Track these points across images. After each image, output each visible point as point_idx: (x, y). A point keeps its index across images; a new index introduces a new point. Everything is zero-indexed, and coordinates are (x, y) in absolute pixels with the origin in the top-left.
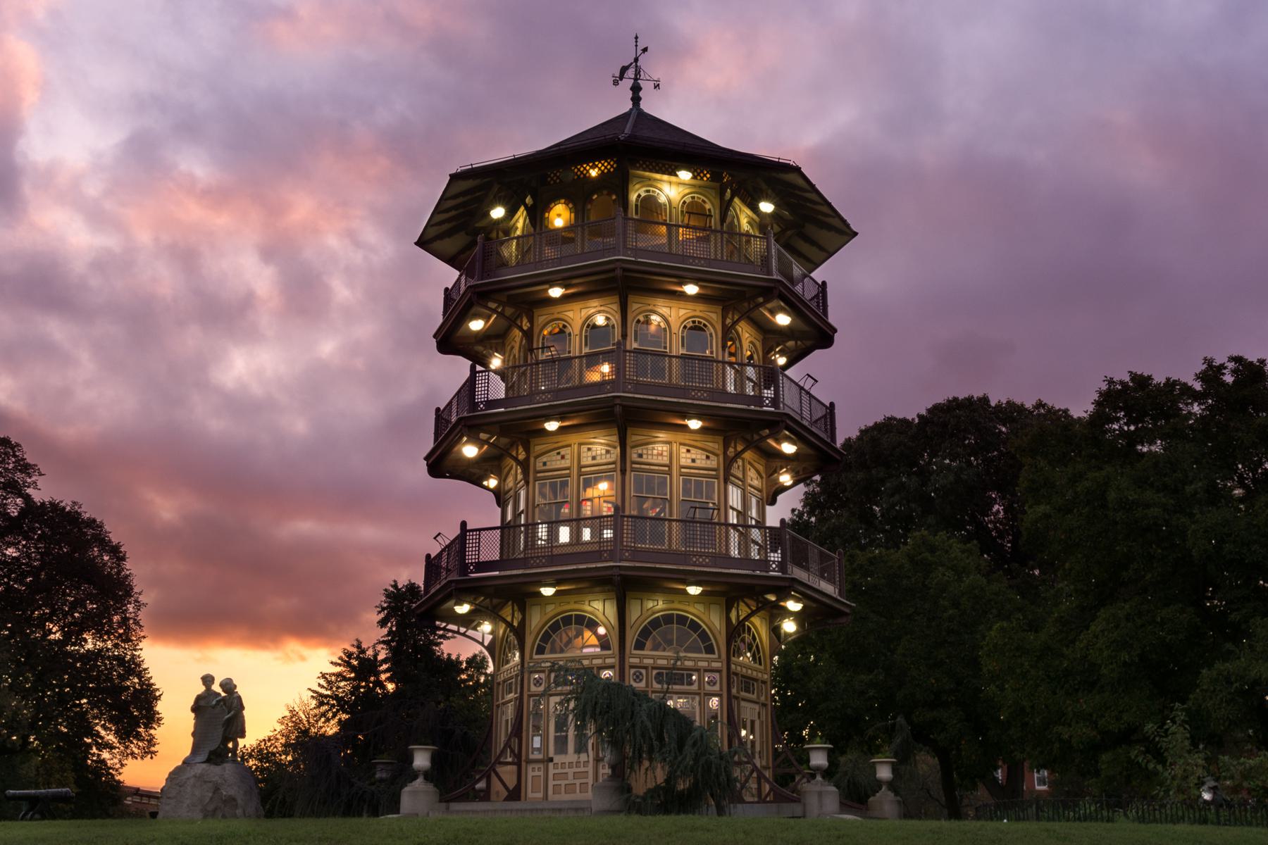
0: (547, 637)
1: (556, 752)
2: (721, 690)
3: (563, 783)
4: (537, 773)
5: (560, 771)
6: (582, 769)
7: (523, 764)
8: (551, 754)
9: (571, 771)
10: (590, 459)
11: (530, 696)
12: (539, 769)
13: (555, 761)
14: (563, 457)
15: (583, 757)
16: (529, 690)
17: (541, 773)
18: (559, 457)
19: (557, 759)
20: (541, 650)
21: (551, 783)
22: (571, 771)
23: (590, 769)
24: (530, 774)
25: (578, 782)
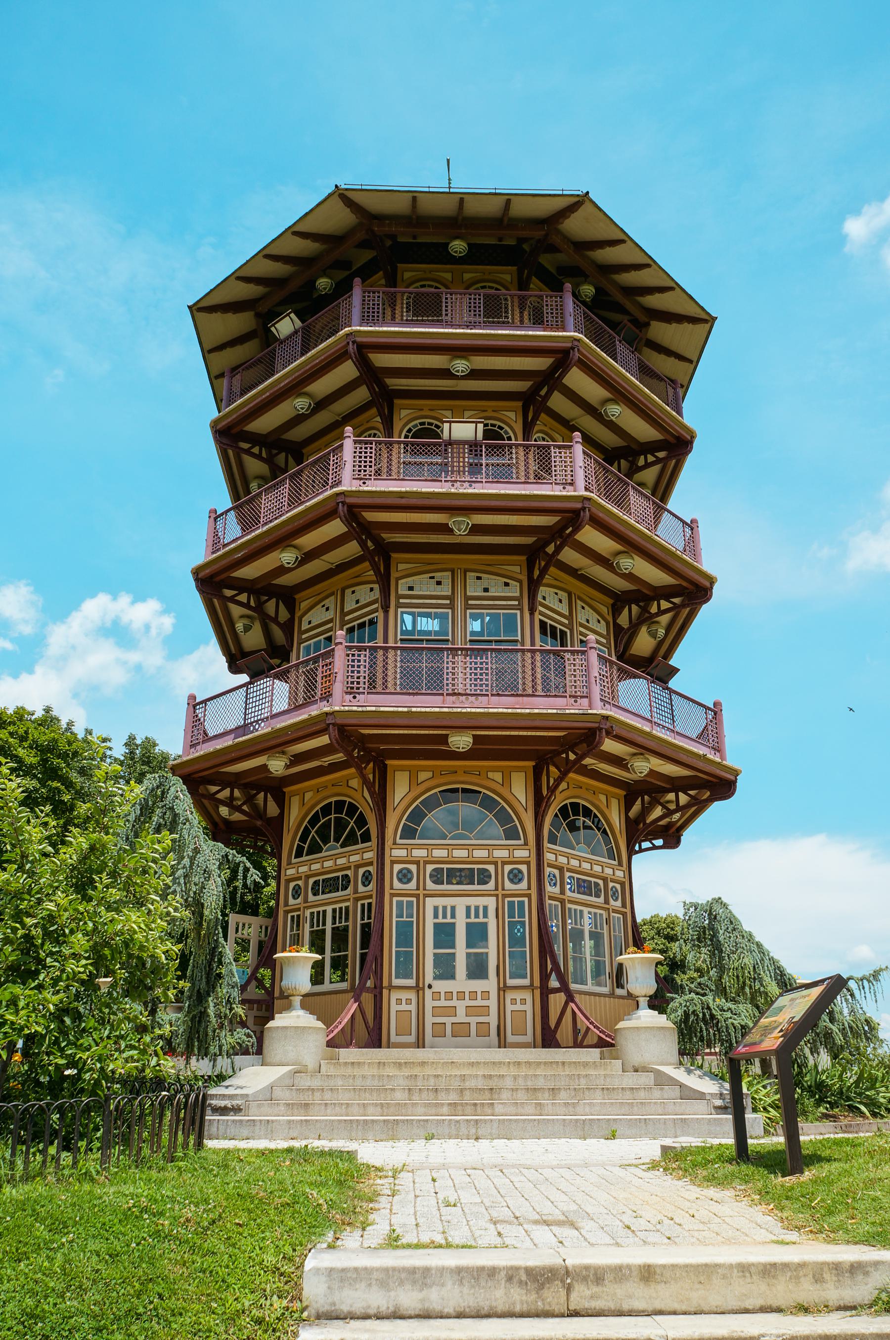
0: (417, 816)
1: (436, 978)
2: (624, 905)
3: (449, 1021)
4: (404, 1007)
5: (443, 1003)
6: (479, 1002)
7: (385, 992)
8: (429, 978)
9: (461, 1006)
10: (481, 589)
11: (392, 895)
12: (409, 1002)
13: (434, 989)
14: (439, 583)
15: (478, 985)
16: (392, 888)
17: (413, 1007)
18: (434, 581)
19: (442, 986)
20: (409, 833)
21: (429, 1020)
22: (461, 1006)
23: (493, 1003)
24: (394, 1008)
25: (473, 1020)
